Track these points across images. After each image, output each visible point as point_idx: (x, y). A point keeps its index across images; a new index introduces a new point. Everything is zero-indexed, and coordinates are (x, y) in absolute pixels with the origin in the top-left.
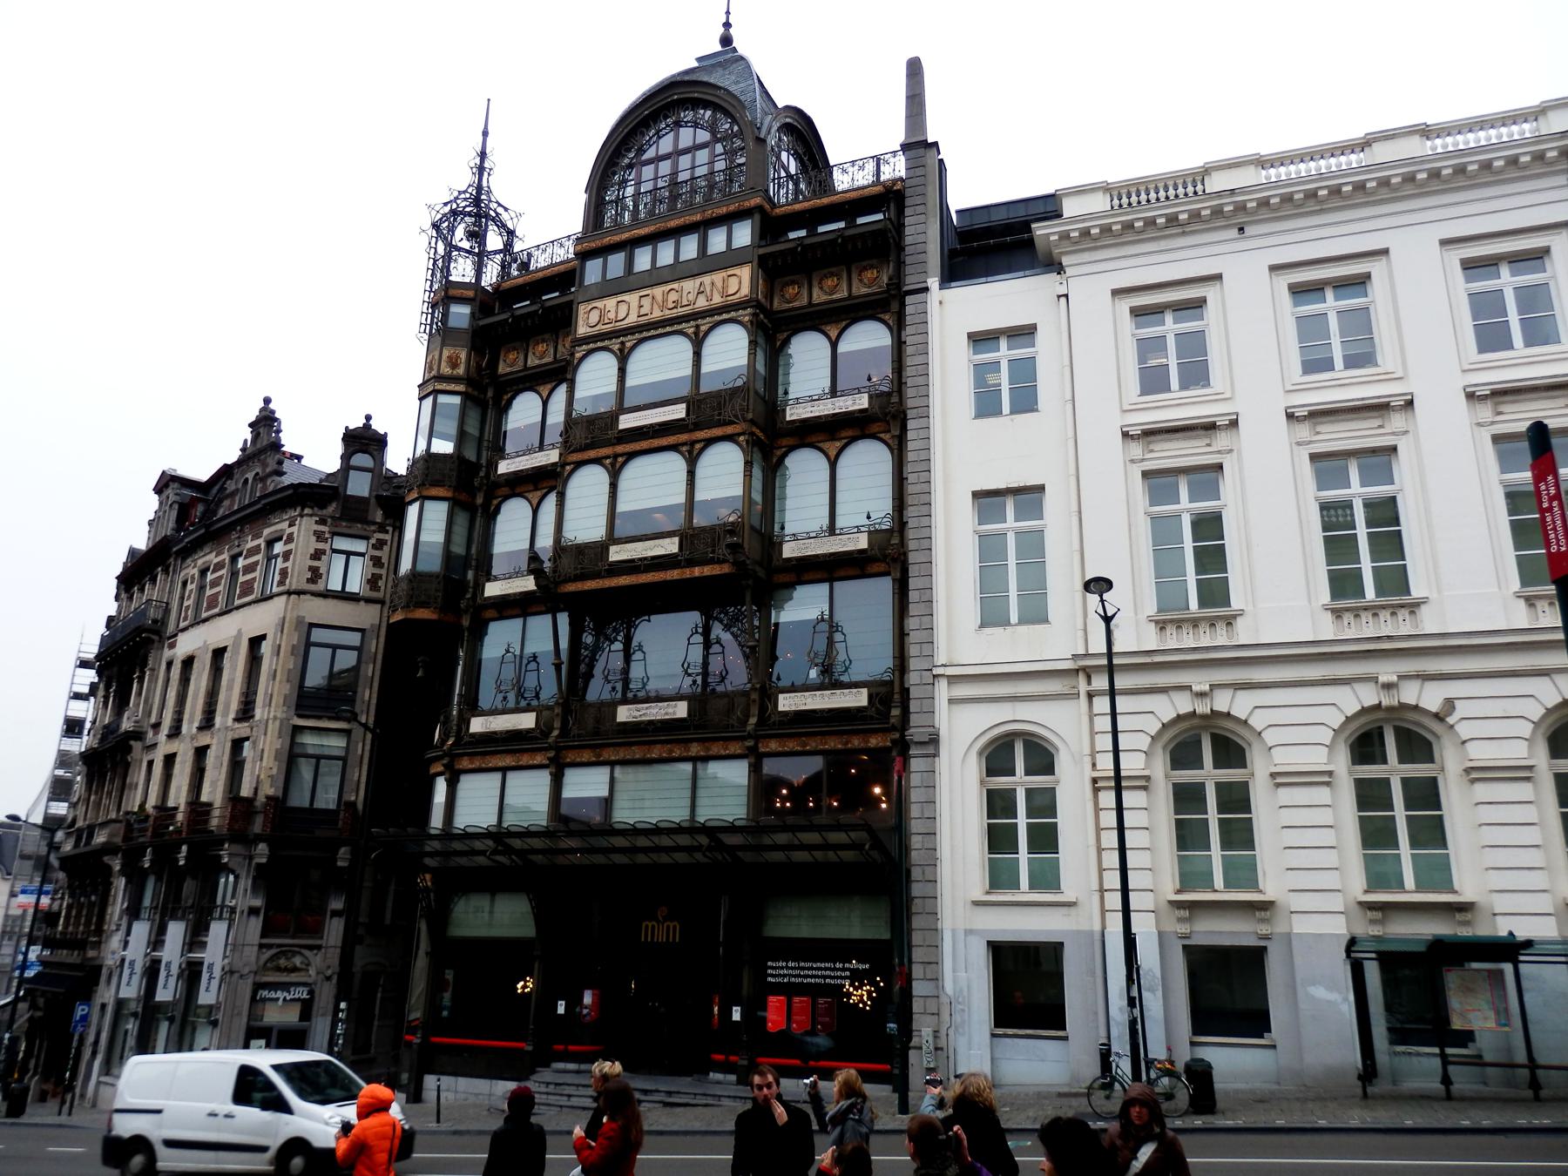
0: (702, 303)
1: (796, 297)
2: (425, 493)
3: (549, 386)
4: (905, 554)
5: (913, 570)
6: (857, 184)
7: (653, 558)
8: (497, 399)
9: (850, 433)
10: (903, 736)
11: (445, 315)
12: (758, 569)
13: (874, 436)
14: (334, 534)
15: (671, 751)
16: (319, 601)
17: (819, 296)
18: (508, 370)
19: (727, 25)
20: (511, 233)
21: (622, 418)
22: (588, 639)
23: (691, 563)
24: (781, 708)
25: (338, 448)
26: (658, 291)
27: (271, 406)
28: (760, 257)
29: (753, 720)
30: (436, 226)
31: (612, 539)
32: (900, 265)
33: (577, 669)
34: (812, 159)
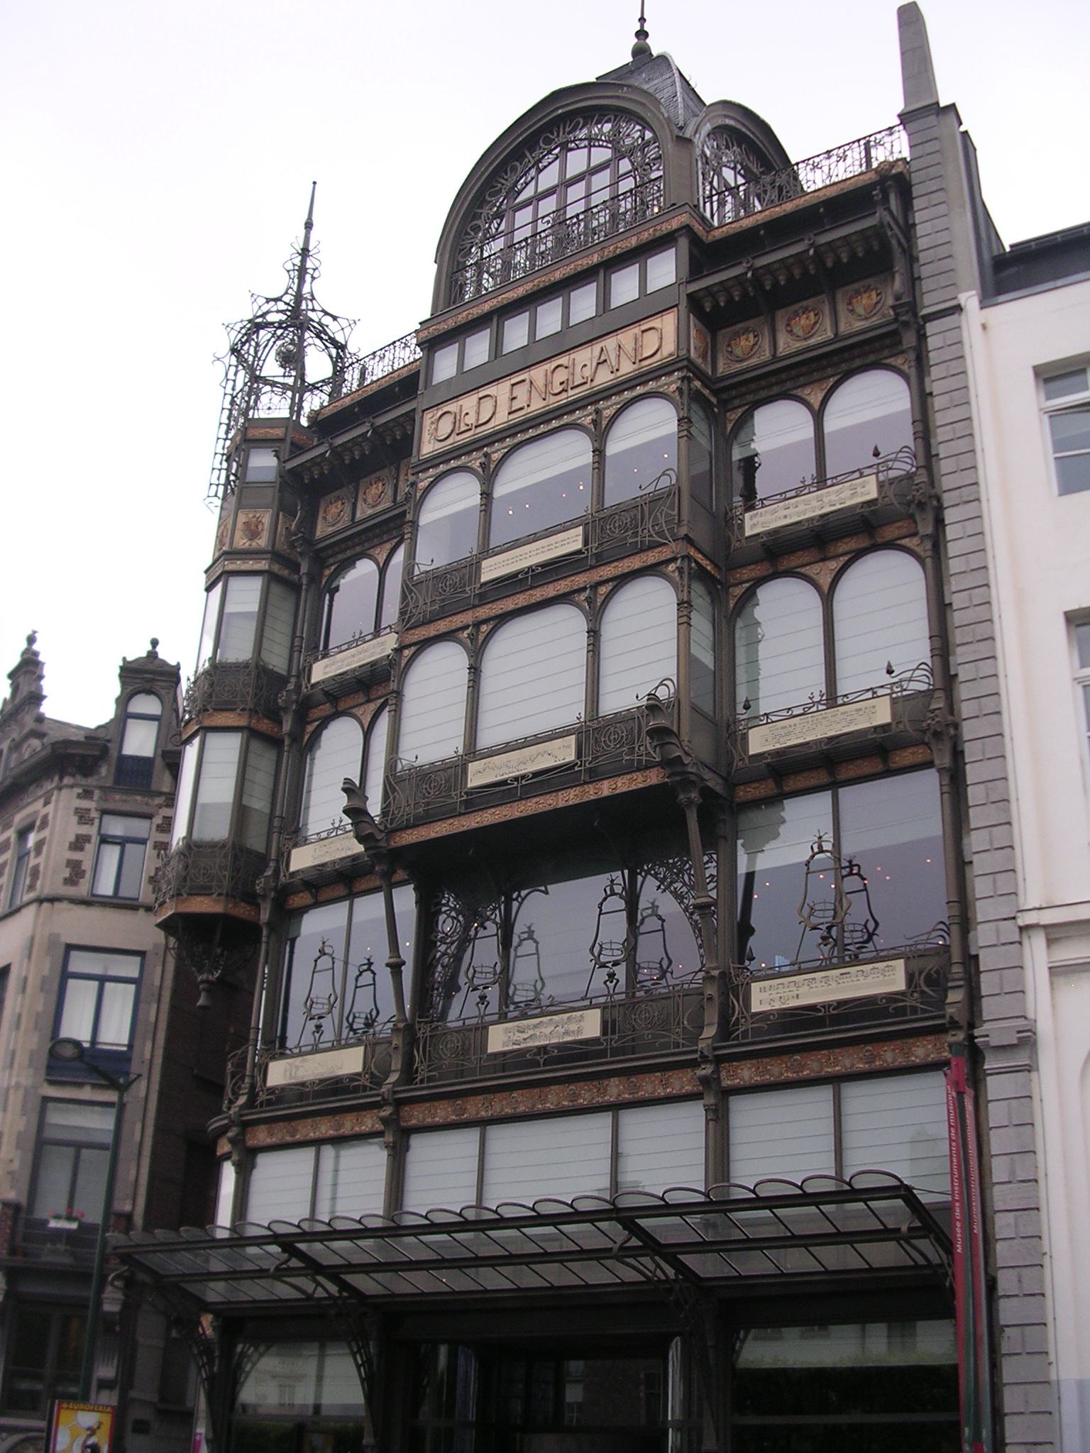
0: (604, 378)
1: (751, 350)
2: (207, 723)
4: (956, 726)
5: (971, 752)
6: (834, 179)
7: (536, 774)
8: (314, 578)
9: (852, 544)
10: (971, 1038)
11: (243, 466)
12: (707, 775)
13: (891, 545)
14: (104, 812)
15: (576, 1096)
16: (81, 911)
17: (787, 344)
18: (330, 530)
20: (342, 347)
21: (485, 564)
22: (446, 925)
23: (595, 775)
24: (756, 1007)
25: (114, 688)
26: (538, 374)
27: (35, 647)
28: (691, 297)
29: (710, 1032)
30: (234, 351)
31: (472, 752)
32: (914, 281)
33: (432, 979)
34: (768, 166)
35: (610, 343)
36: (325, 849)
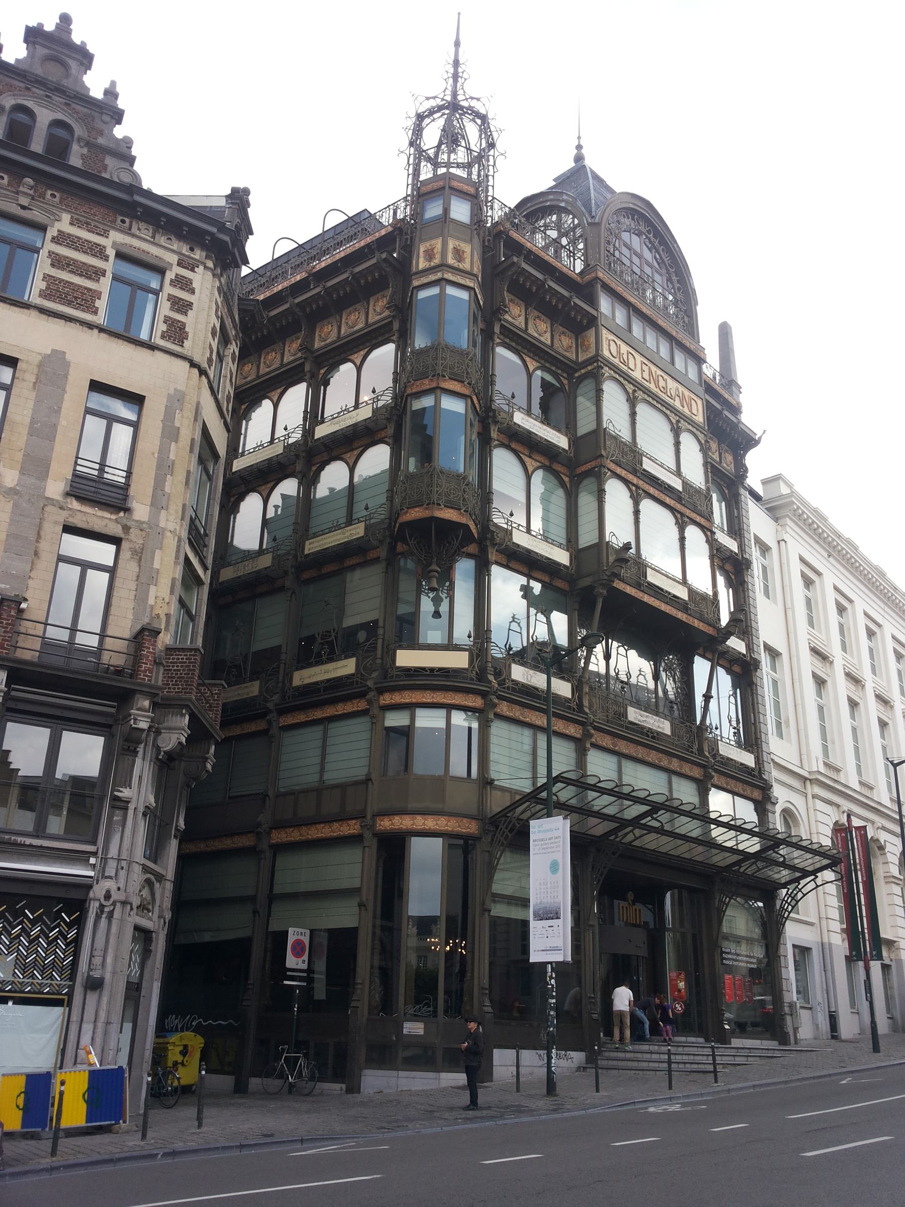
0: (677, 404)
3: (536, 364)
7: (675, 596)
19: (579, 147)
26: (654, 368)
35: (681, 389)
36: (535, 543)
